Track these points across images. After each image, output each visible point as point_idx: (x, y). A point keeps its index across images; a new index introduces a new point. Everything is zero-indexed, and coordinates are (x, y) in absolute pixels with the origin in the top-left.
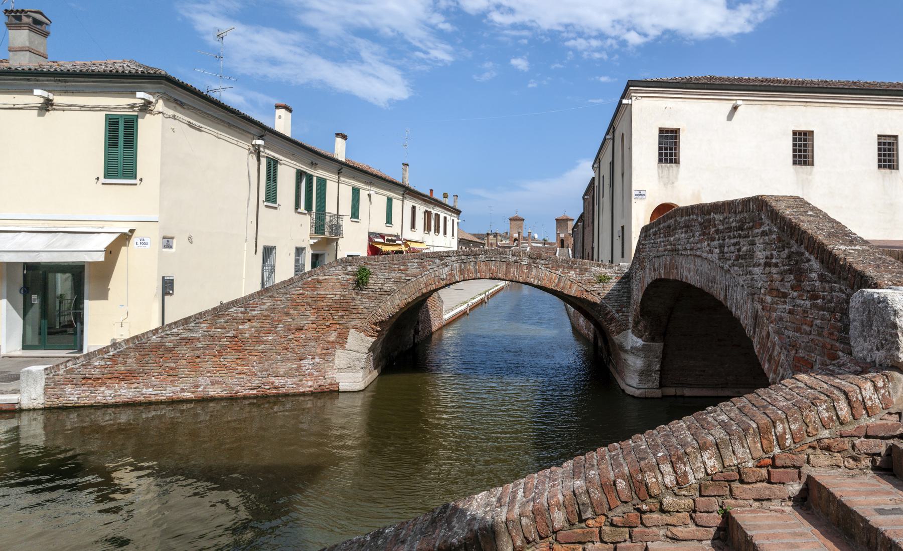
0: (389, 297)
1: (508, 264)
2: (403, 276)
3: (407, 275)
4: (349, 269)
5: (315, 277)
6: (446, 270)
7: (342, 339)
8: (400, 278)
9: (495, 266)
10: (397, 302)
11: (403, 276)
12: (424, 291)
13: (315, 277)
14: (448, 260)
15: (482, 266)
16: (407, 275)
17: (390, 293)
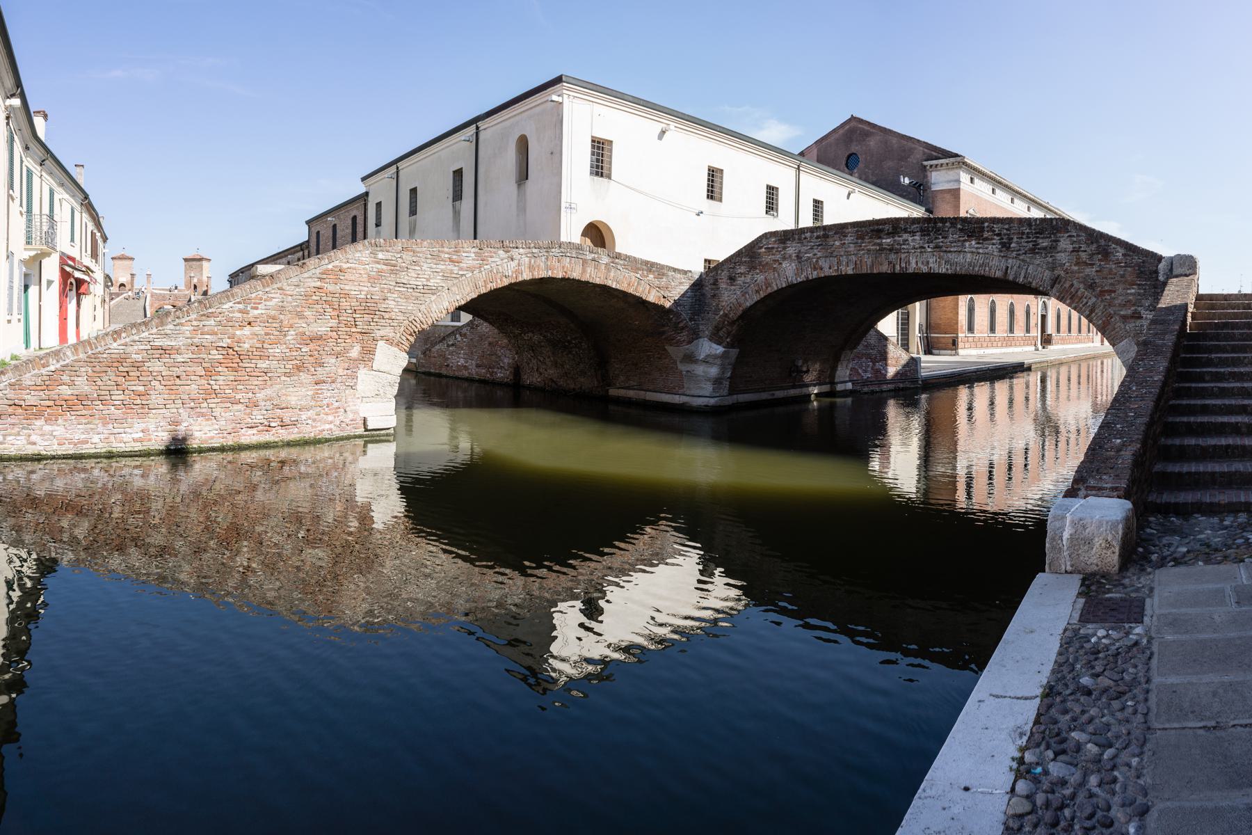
0: (433, 298)
1: (585, 262)
2: (456, 270)
3: (461, 269)
4: (380, 256)
5: (337, 263)
6: (514, 264)
7: (368, 354)
10: (446, 304)
11: (456, 270)
12: (483, 291)
13: (337, 263)
14: (515, 253)
15: (554, 262)
16: (461, 269)
17: (434, 291)
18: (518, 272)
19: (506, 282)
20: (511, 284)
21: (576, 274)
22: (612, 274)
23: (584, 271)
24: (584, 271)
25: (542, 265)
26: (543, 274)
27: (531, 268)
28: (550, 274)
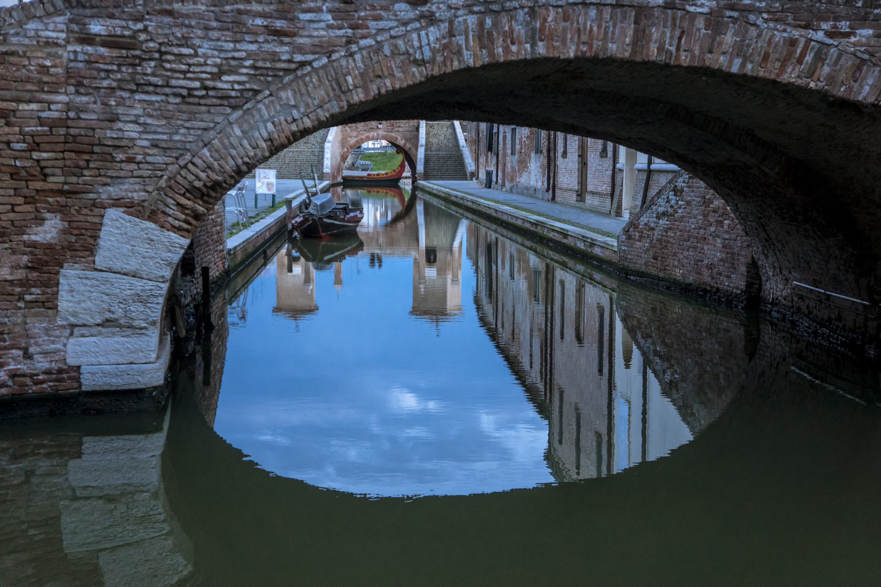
2: (284, 51)
3: (300, 49)
6: (434, 32)
8: (274, 57)
9: (599, 18)
11: (284, 51)
12: (358, 96)
16: (300, 49)
18: (449, 49)
19: (417, 74)
20: (431, 79)
21: (619, 46)
22: (729, 38)
23: (640, 37)
24: (640, 37)
25: (520, 30)
26: (521, 51)
27: (484, 38)
28: (541, 49)
